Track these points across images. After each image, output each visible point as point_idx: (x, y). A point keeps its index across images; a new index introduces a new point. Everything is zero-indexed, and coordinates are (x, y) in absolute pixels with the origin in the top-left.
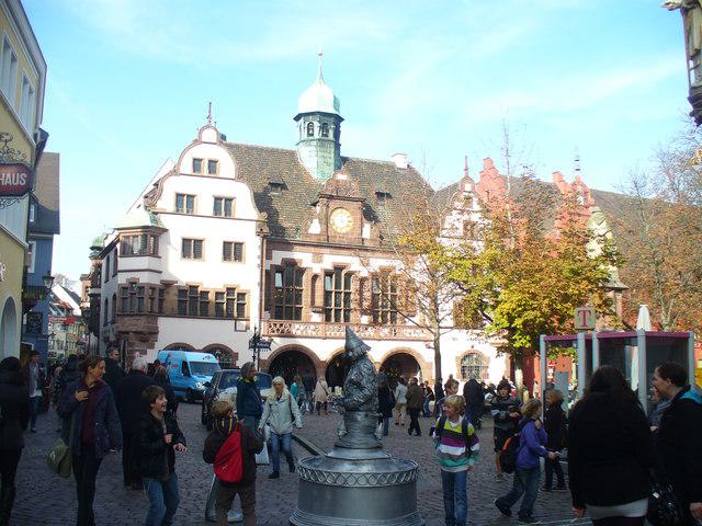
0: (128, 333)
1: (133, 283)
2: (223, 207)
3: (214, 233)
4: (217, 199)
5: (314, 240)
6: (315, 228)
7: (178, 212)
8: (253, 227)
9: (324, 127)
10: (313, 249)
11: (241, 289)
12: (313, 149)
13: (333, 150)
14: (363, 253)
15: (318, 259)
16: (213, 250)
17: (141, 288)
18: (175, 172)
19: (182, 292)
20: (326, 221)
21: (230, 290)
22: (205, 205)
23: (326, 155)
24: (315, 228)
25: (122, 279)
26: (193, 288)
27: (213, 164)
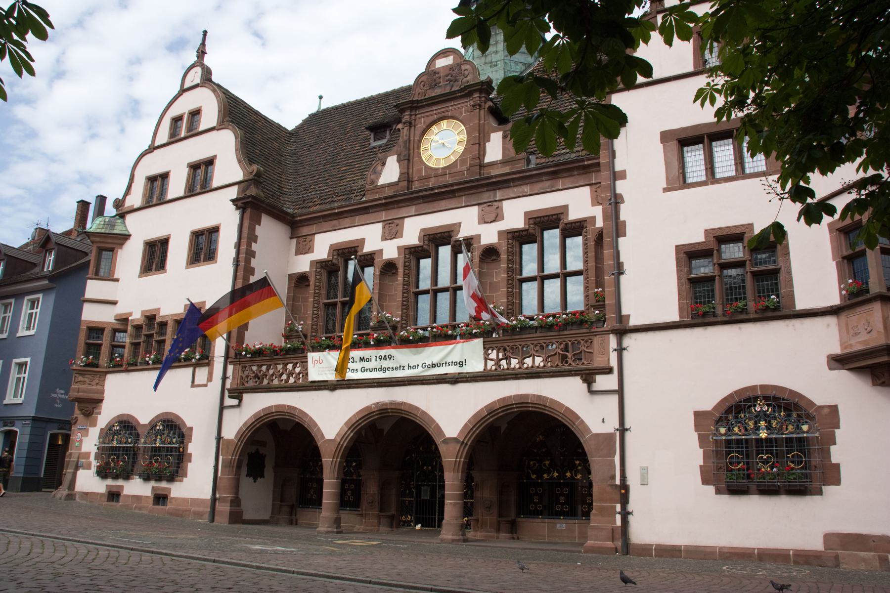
3: (177, 222)
4: (194, 167)
6: (390, 172)
7: (148, 204)
10: (384, 215)
14: (486, 197)
15: (392, 231)
18: (152, 149)
19: (138, 328)
20: (409, 157)
24: (390, 172)
27: (196, 113)
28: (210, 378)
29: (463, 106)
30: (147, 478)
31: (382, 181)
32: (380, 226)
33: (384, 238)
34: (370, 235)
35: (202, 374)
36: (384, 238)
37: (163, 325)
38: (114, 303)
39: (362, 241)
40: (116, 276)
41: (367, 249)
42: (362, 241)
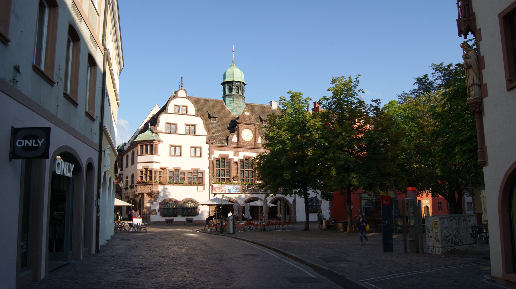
0: (143, 194)
1: (146, 169)
2: (192, 130)
3: (187, 142)
5: (235, 145)
8: (205, 139)
9: (238, 88)
11: (201, 169)
12: (232, 99)
13: (241, 100)
15: (236, 154)
16: (186, 151)
17: (151, 172)
20: (239, 136)
21: (196, 171)
22: (181, 129)
23: (238, 102)
24: (234, 139)
25: (140, 167)
26: (177, 170)
28: (204, 189)
29: (253, 127)
30: (183, 216)
31: (232, 141)
32: (233, 153)
33: (234, 156)
34: (230, 154)
35: (200, 188)
36: (234, 156)
37: (183, 173)
38: (159, 163)
39: (228, 155)
40: (159, 154)
41: (230, 157)
42: (228, 155)
